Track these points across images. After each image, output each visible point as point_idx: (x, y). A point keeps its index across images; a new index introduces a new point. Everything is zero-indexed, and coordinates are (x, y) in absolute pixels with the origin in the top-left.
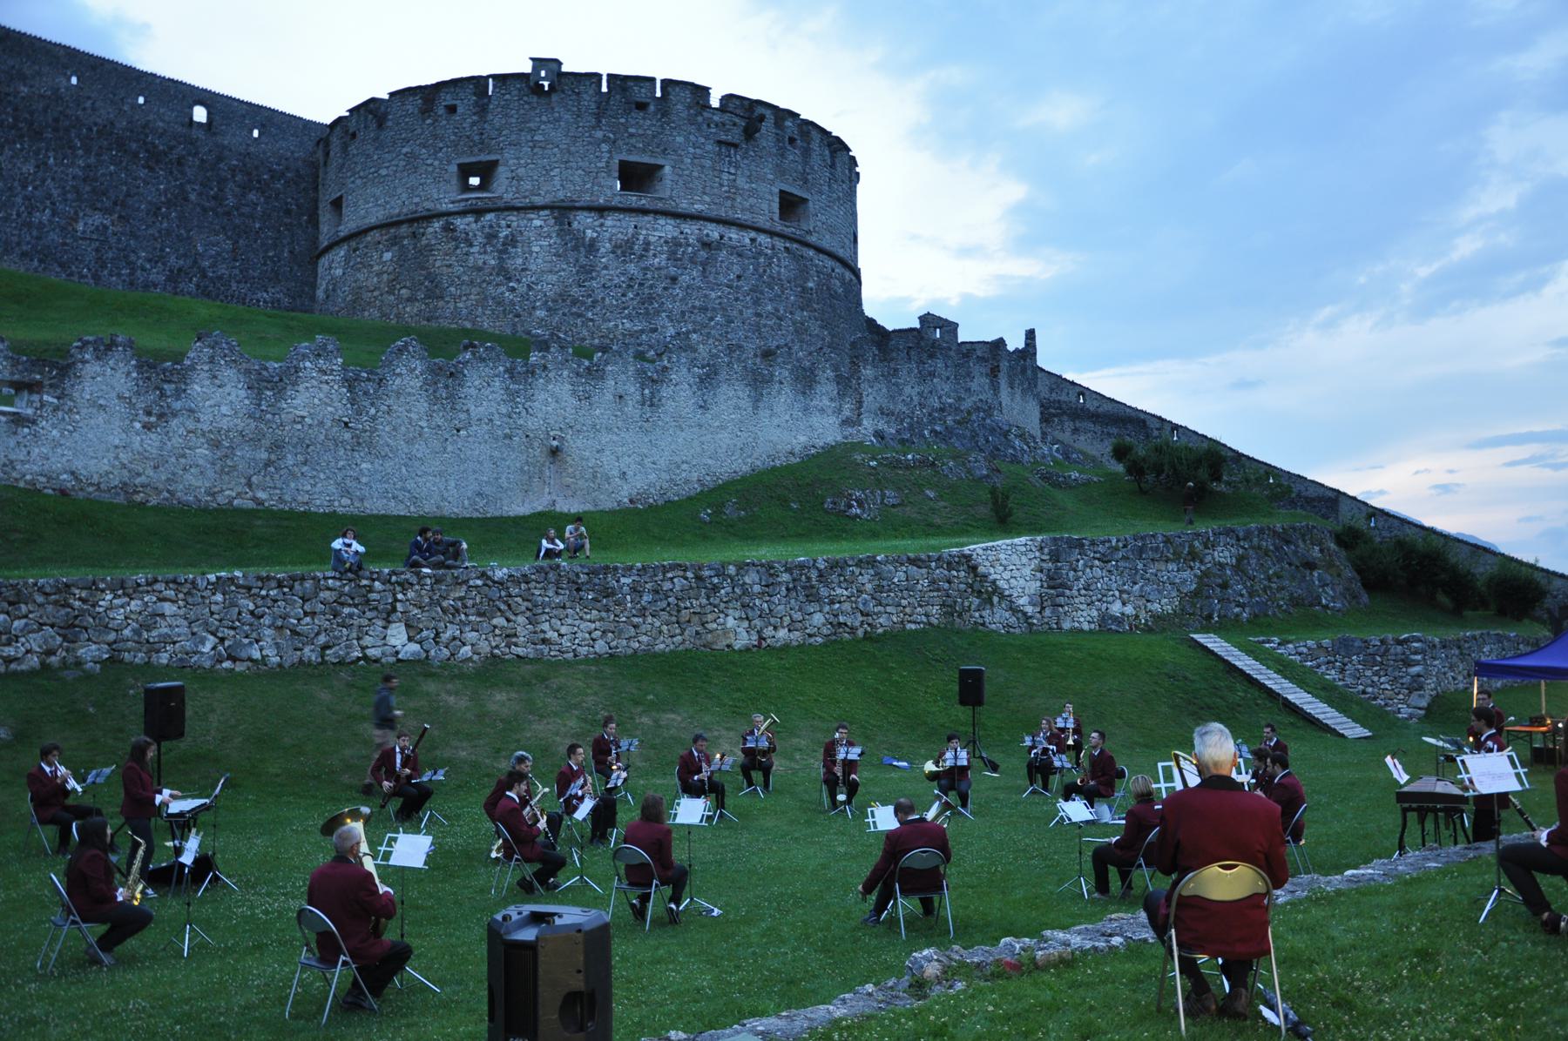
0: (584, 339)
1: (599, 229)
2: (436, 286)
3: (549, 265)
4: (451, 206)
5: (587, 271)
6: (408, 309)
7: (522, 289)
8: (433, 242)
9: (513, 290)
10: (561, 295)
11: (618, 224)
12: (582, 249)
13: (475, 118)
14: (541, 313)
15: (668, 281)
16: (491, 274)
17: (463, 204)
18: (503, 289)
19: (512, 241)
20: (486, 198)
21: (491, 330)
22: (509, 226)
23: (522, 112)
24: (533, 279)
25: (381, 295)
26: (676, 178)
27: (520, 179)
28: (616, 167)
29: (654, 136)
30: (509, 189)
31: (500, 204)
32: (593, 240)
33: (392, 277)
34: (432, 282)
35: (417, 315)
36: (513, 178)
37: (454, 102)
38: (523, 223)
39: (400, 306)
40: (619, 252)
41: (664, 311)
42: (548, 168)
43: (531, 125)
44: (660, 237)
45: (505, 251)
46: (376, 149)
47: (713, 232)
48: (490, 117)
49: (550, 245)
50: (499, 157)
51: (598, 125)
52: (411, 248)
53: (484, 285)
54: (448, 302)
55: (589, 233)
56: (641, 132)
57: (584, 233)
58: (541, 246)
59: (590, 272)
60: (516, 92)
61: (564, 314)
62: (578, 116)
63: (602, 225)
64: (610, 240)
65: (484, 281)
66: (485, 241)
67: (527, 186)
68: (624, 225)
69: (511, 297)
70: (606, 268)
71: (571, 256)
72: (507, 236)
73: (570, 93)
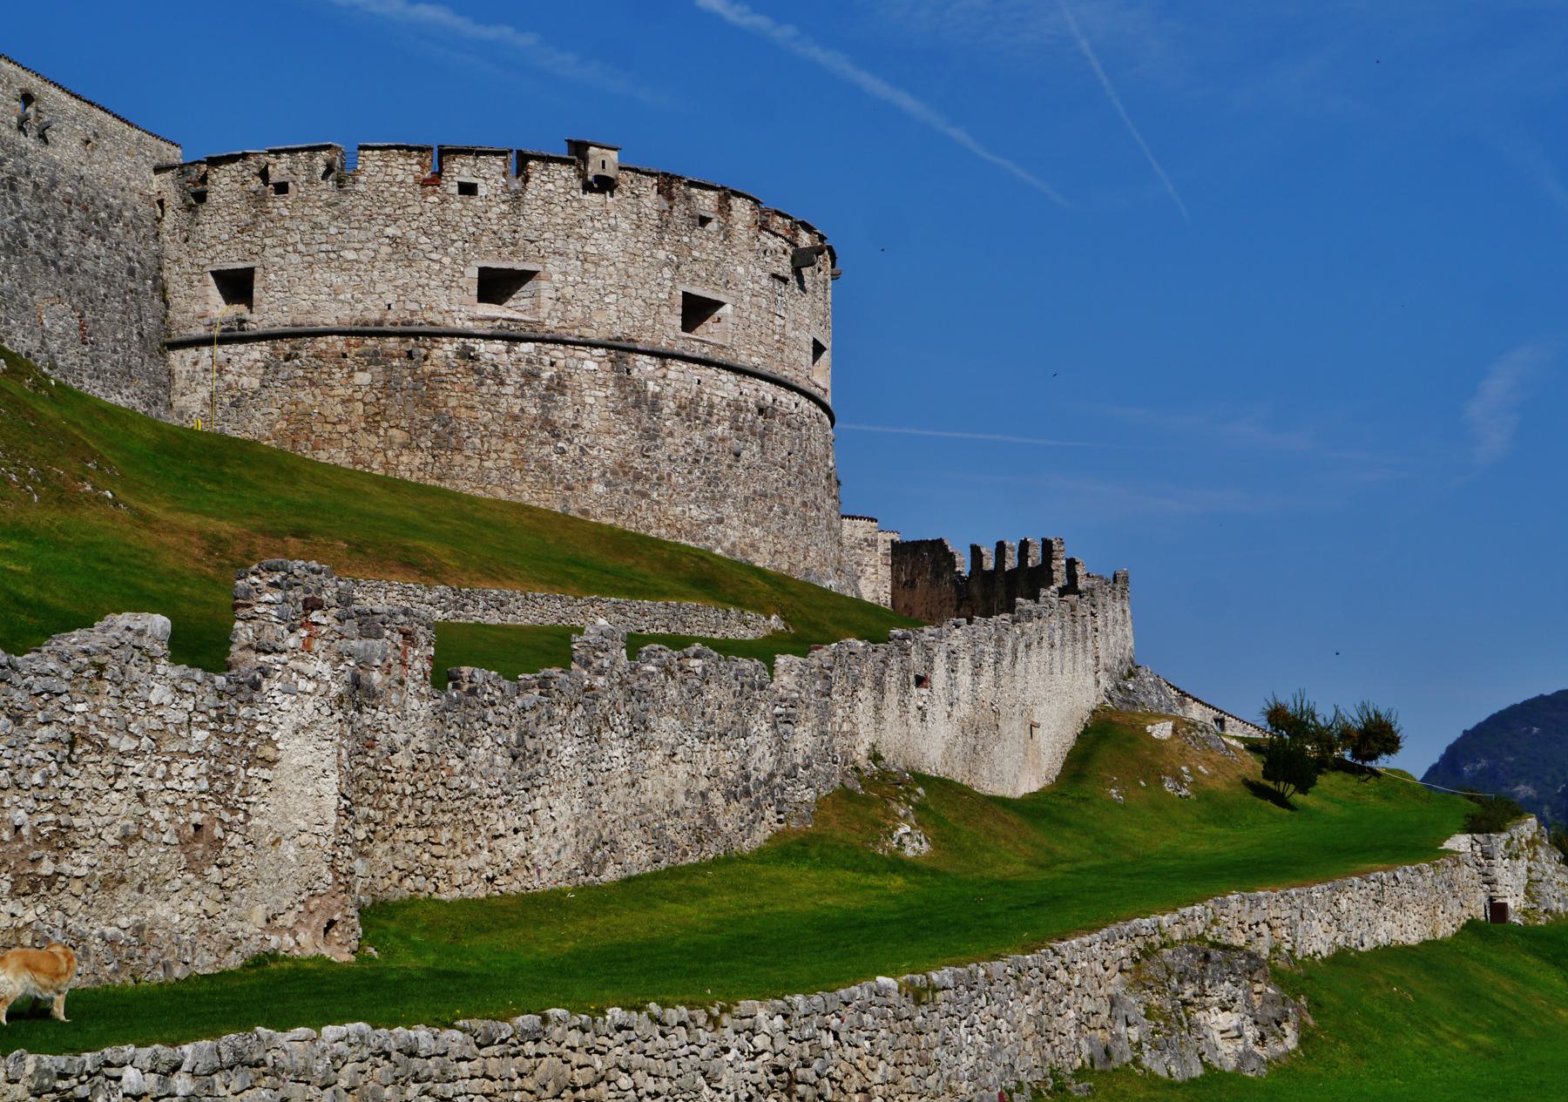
0: (649, 528)
1: (661, 381)
2: (451, 433)
3: (606, 424)
4: (470, 324)
5: (651, 435)
6: (404, 459)
7: (573, 452)
8: (444, 371)
9: (563, 452)
10: (621, 466)
11: (681, 375)
12: (644, 407)
13: (504, 207)
14: (598, 488)
15: (732, 456)
16: (532, 427)
17: (489, 324)
18: (547, 449)
19: (559, 385)
20: (522, 321)
21: (535, 504)
22: (552, 364)
23: (569, 210)
24: (587, 440)
25: (353, 431)
26: (737, 321)
27: (567, 302)
28: (680, 301)
29: (717, 265)
30: (553, 314)
31: (541, 333)
32: (656, 396)
33: (371, 410)
34: (444, 426)
35: (420, 470)
36: (558, 300)
37: (474, 180)
38: (571, 362)
39: (390, 453)
40: (684, 414)
41: (730, 496)
42: (602, 291)
43: (583, 231)
44: (723, 398)
45: (550, 399)
46: (336, 218)
47: (768, 391)
48: (526, 209)
49: (606, 397)
50: (540, 268)
51: (659, 243)
52: (406, 373)
53: (523, 441)
54: (468, 458)
55: (651, 386)
56: (704, 256)
57: (646, 385)
58: (596, 397)
59: (654, 438)
60: (561, 183)
61: (626, 492)
62: (638, 227)
63: (664, 377)
64: (674, 397)
65: (523, 436)
66: (522, 380)
67: (576, 312)
68: (688, 380)
69: (560, 462)
70: (671, 434)
71: (633, 414)
72: (551, 379)
73: (629, 194)
